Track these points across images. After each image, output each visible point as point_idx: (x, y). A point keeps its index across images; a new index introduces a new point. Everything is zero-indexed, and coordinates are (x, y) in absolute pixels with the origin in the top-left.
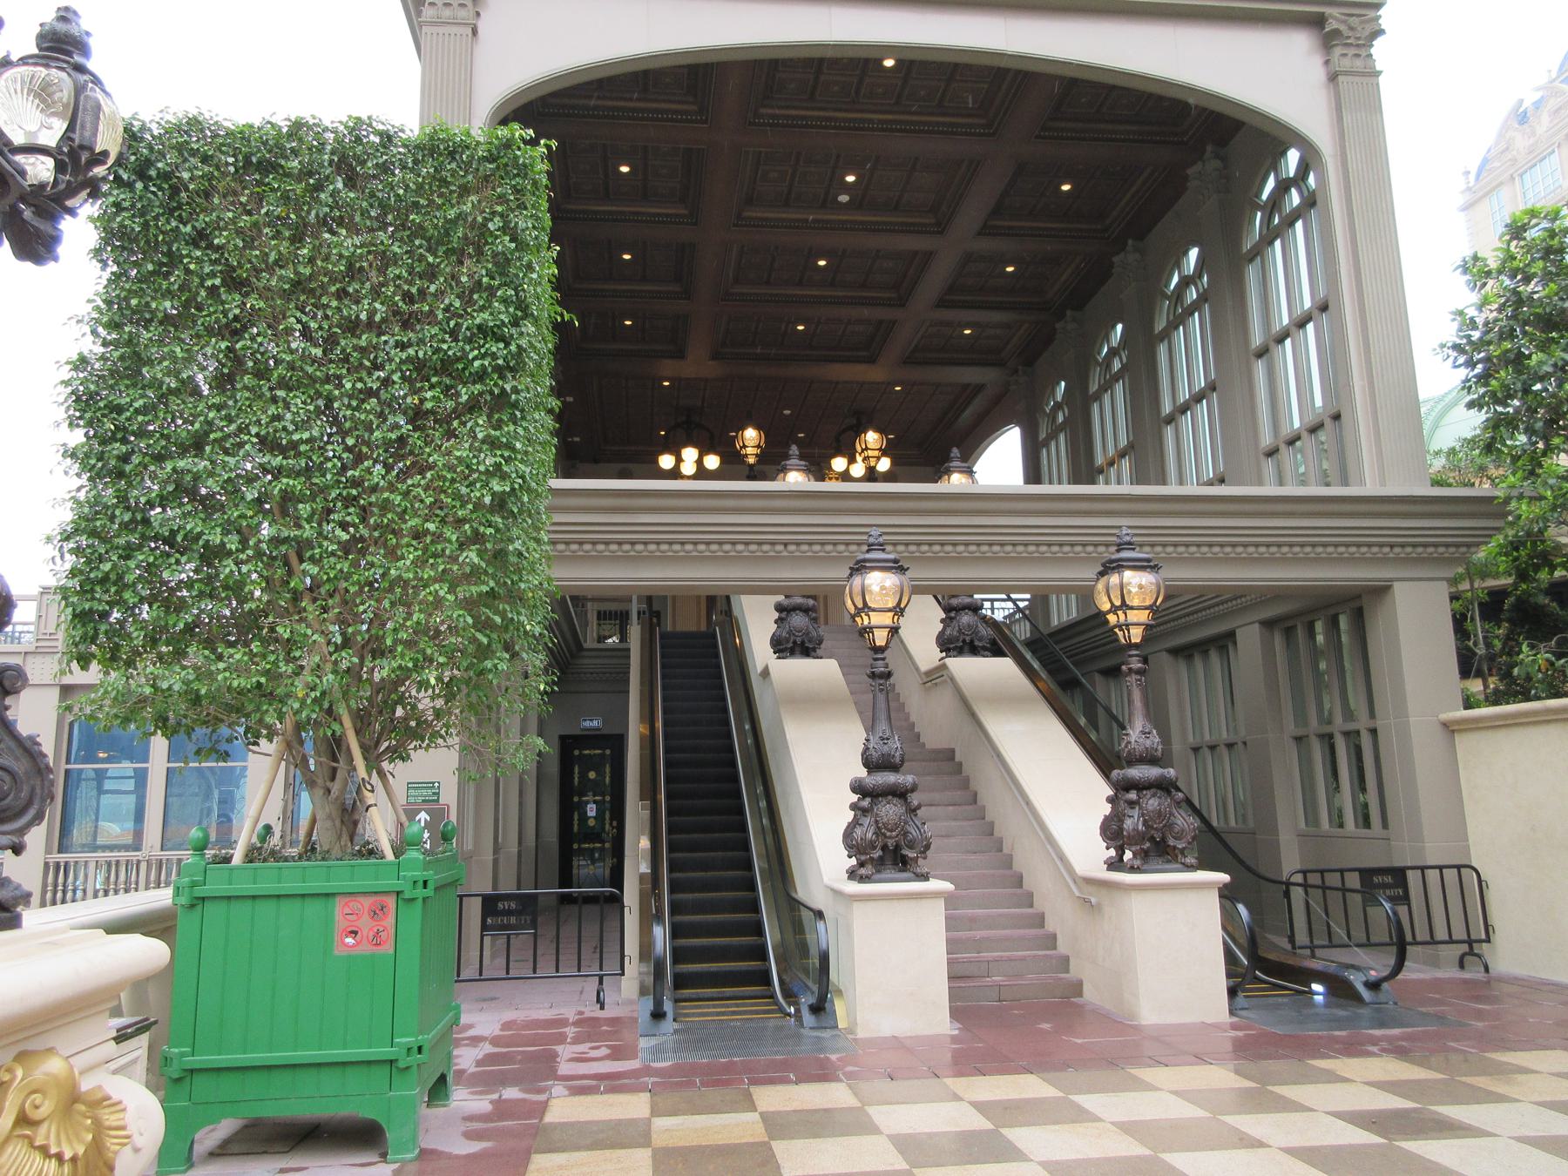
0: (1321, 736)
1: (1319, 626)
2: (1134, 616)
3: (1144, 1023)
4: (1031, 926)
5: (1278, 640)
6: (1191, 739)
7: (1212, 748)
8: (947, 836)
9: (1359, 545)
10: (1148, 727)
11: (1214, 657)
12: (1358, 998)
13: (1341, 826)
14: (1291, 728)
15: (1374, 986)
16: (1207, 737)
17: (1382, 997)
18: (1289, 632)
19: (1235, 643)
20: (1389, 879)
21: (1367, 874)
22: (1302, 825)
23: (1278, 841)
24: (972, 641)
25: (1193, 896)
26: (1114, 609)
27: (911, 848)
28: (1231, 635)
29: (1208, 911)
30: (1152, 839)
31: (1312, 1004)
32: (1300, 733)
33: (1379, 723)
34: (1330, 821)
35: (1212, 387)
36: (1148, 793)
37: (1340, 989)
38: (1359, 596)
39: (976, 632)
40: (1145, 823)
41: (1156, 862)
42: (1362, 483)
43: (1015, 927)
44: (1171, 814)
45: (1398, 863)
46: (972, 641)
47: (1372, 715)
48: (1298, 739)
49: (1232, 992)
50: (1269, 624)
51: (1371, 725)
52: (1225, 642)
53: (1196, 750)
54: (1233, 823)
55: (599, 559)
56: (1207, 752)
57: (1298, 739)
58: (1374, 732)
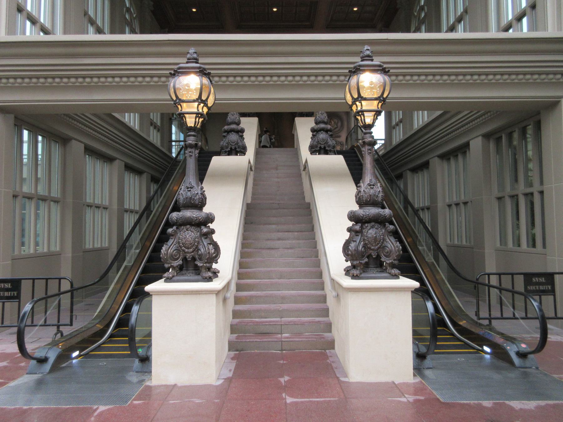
0: (512, 197)
1: (516, 135)
2: (366, 105)
3: (352, 380)
4: (319, 302)
5: (492, 145)
6: (447, 201)
7: (457, 204)
8: (291, 248)
9: (540, 74)
10: (374, 181)
11: (460, 158)
12: (511, 362)
13: (519, 246)
14: (496, 193)
15: (522, 355)
16: (455, 199)
17: (528, 363)
18: (498, 140)
19: (469, 149)
20: (543, 280)
21: (528, 277)
22: (498, 244)
23: (484, 253)
24: (325, 148)
25: (392, 297)
26: (355, 101)
27: (200, 259)
28: (467, 145)
29: (405, 305)
30: (369, 257)
31: (482, 358)
32: (500, 195)
33: (545, 188)
34: (513, 243)
35: (466, 11)
36: (369, 225)
37: (500, 353)
38: (539, 113)
39: (327, 143)
40: (365, 246)
41: (373, 272)
42: (545, 29)
43: (308, 302)
44: (384, 240)
45: (550, 270)
46: (325, 148)
47: (542, 183)
48: (499, 199)
49: (420, 357)
50: (487, 136)
51: (540, 189)
52: (464, 148)
53: (450, 206)
54: (464, 243)
55: (66, 88)
56: (454, 207)
57: (499, 199)
58: (542, 193)
